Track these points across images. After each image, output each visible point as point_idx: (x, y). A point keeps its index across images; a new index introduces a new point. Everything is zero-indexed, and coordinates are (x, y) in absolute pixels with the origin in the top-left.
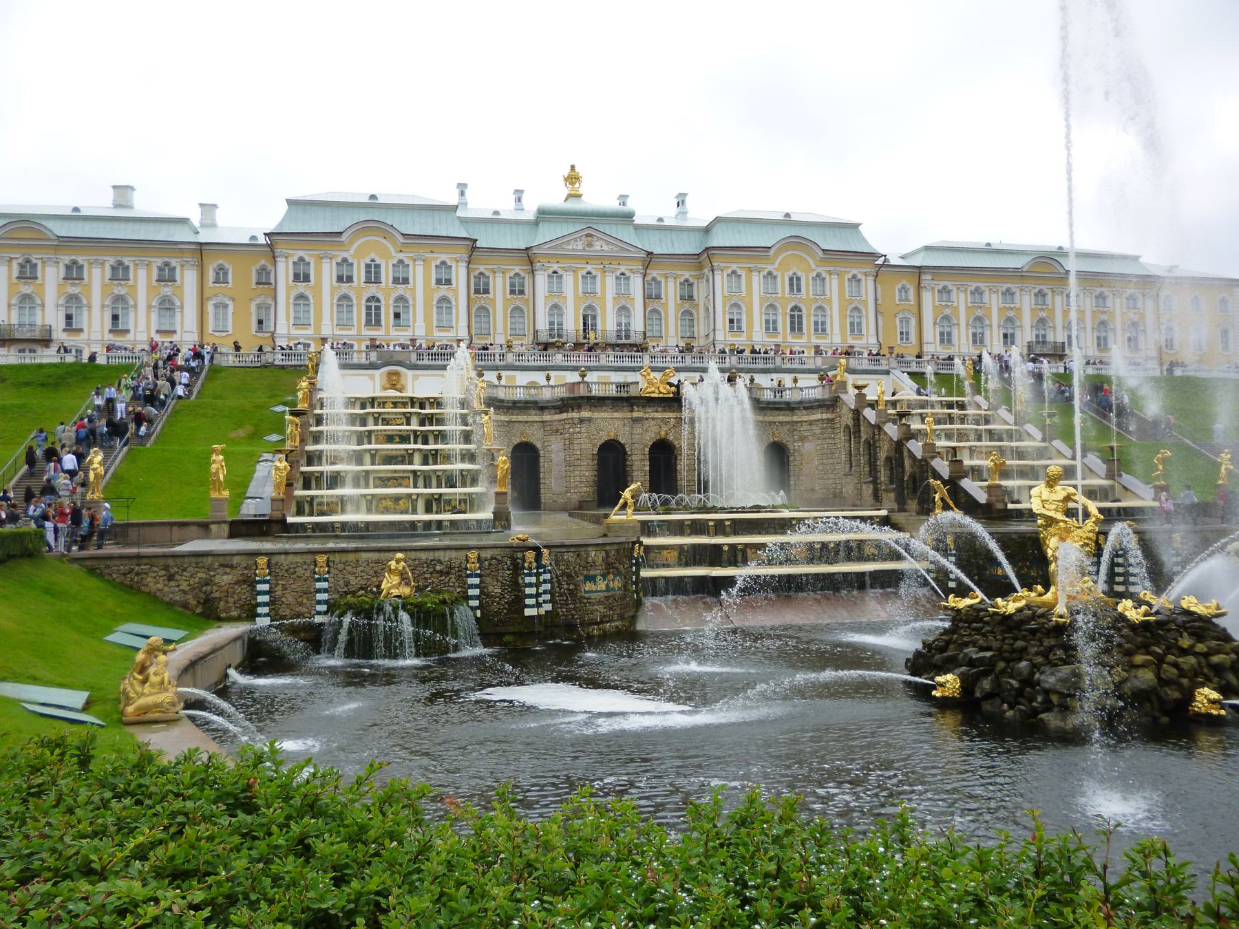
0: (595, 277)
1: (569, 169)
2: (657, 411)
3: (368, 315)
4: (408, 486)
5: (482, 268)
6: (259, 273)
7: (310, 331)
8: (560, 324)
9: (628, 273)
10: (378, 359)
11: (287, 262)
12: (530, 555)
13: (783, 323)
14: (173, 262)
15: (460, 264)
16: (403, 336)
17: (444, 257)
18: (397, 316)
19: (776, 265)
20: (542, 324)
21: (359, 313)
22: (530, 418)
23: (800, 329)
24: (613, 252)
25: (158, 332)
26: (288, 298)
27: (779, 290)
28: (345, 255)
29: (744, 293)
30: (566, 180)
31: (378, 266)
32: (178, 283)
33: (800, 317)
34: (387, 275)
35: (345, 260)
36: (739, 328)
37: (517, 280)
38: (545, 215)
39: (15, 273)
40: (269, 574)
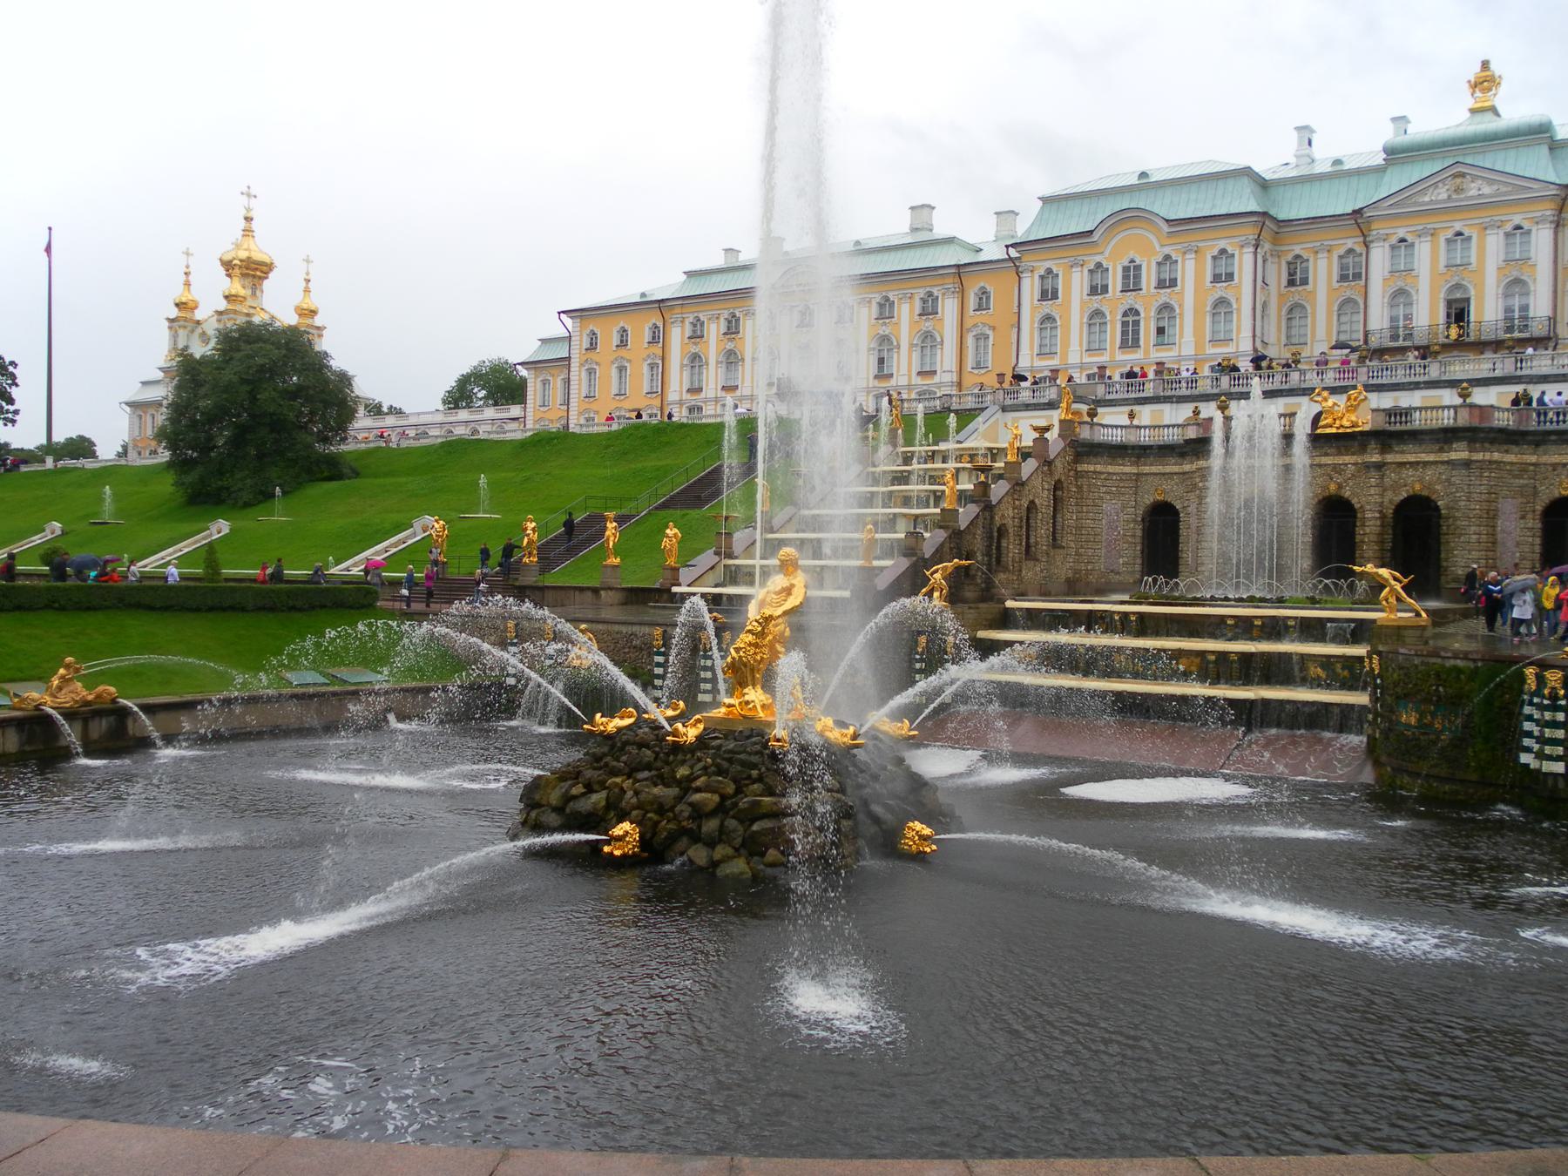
0: (1469, 238)
1: (1478, 68)
2: (1326, 455)
3: (1124, 333)
5: (1297, 252)
7: (1054, 362)
8: (1408, 317)
11: (1032, 277)
14: (936, 292)
15: (1245, 250)
18: (1160, 331)
20: (1378, 320)
21: (1114, 332)
22: (1168, 469)
24: (1505, 194)
25: (919, 373)
26: (1032, 322)
28: (1098, 258)
31: (1138, 268)
32: (939, 315)
34: (1149, 278)
35: (1099, 265)
37: (1350, 260)
38: (1396, 155)
39: (918, 310)
40: (516, 637)
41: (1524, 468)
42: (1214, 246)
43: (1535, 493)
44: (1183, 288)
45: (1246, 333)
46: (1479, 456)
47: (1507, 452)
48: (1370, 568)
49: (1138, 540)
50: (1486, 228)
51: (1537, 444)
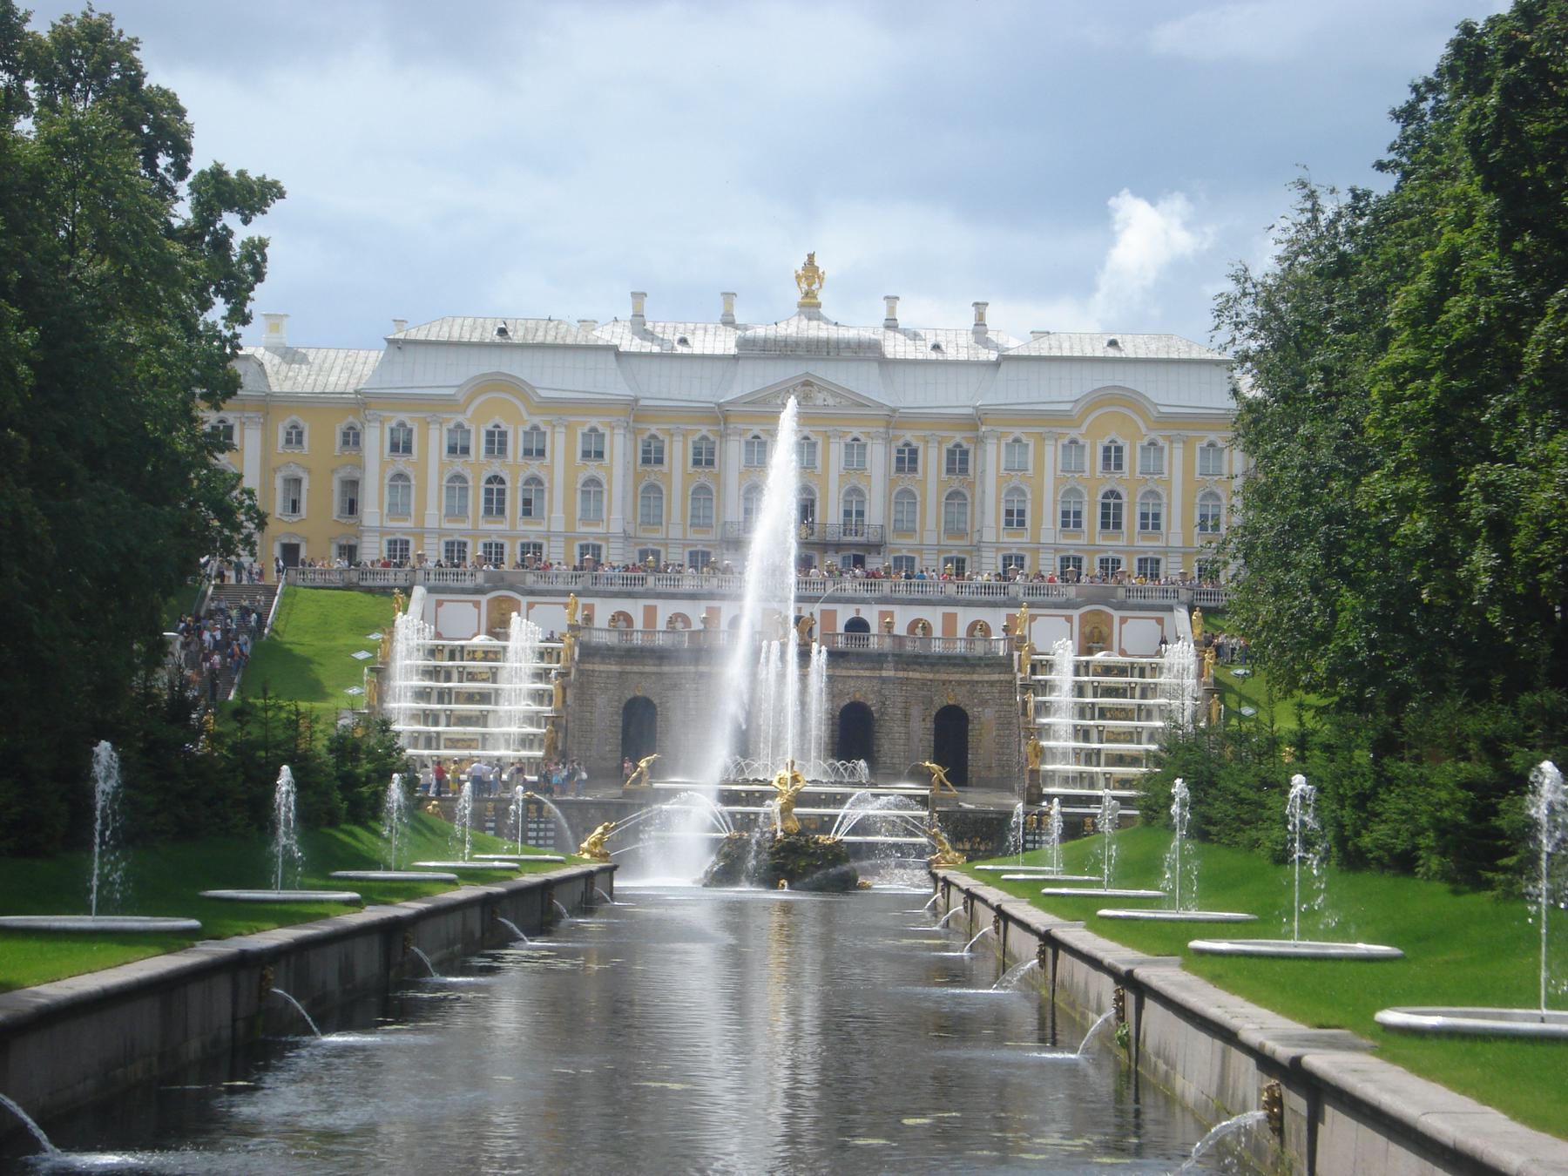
3: (488, 501)
4: (476, 748)
6: (346, 435)
7: (409, 524)
9: (863, 439)
10: (486, 582)
12: (533, 807)
13: (1091, 515)
16: (531, 530)
17: (594, 422)
19: (1084, 429)
22: (648, 669)
23: (1118, 525)
26: (382, 478)
27: (1087, 466)
28: (460, 418)
29: (1031, 471)
30: (798, 277)
31: (503, 434)
33: (1118, 507)
34: (515, 445)
35: (460, 426)
36: (1021, 523)
41: (924, 683)
42: (584, 423)
43: (932, 701)
44: (552, 461)
45: (616, 515)
46: (901, 674)
47: (914, 670)
48: (927, 764)
49: (620, 730)
50: (829, 437)
51: (932, 665)
